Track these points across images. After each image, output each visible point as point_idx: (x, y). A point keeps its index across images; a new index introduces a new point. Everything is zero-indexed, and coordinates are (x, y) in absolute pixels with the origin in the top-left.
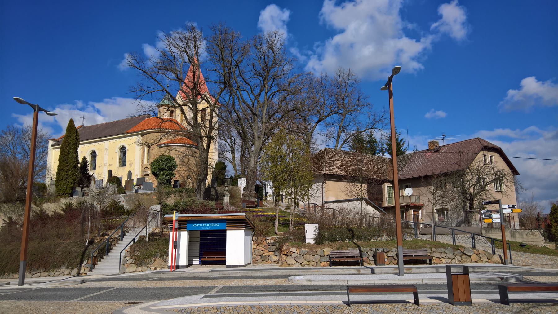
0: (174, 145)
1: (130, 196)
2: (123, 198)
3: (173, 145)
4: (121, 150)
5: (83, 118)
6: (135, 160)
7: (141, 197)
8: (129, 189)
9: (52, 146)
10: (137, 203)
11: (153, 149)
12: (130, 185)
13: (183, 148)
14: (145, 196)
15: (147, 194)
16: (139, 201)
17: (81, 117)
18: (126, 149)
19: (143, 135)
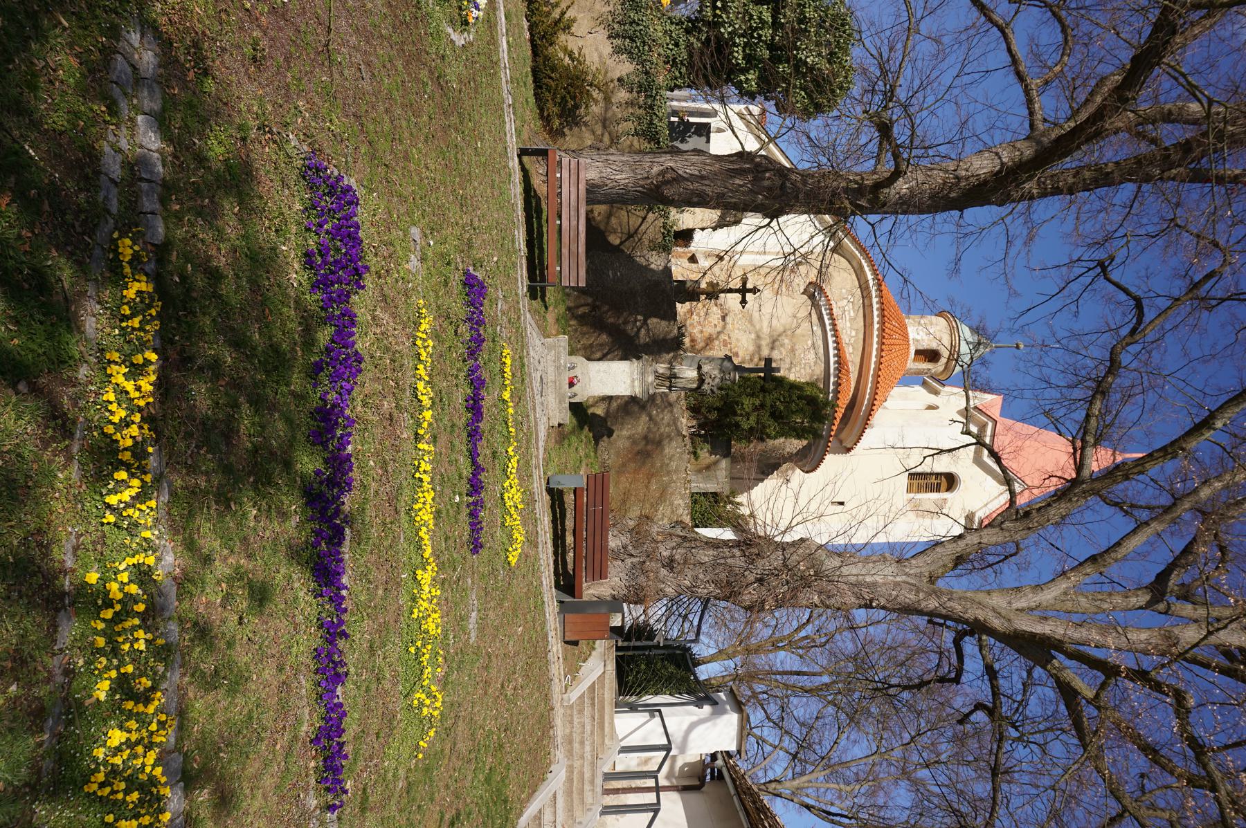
0: (828, 328)
3: (827, 322)
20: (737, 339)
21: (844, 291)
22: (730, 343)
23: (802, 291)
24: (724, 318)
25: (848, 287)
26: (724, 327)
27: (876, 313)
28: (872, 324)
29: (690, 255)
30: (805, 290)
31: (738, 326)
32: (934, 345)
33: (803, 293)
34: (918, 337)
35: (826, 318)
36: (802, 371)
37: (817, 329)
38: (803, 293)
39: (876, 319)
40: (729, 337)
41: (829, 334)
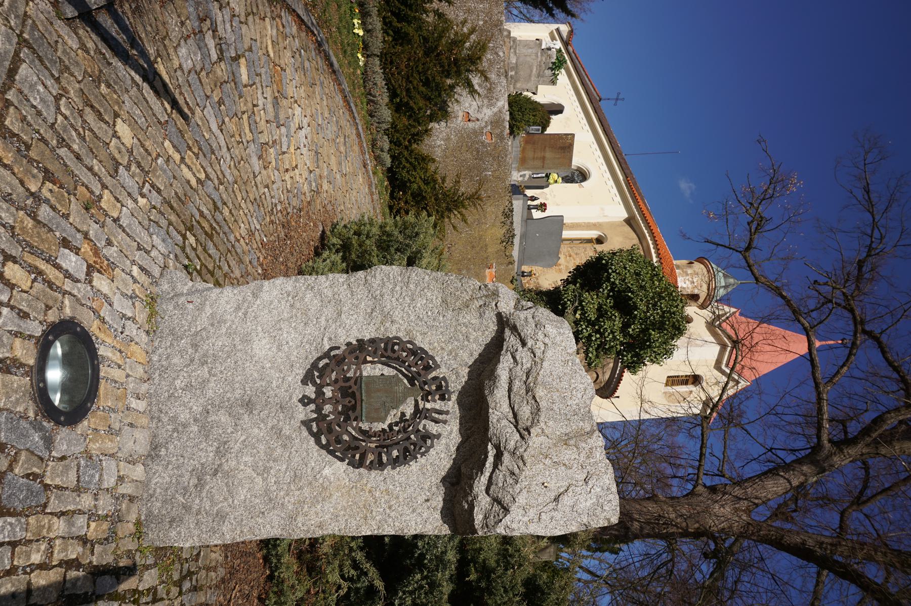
1: (499, 157)
2: (487, 113)
4: (577, 170)
5: (617, 99)
6: (557, 205)
7: (492, 211)
8: (530, 154)
9: (558, 30)
10: (464, 188)
12: (548, 154)
14: (500, 232)
15: (508, 239)
16: (475, 198)
17: (619, 94)
18: (581, 181)
19: (630, 222)
32: (696, 292)
34: (685, 286)
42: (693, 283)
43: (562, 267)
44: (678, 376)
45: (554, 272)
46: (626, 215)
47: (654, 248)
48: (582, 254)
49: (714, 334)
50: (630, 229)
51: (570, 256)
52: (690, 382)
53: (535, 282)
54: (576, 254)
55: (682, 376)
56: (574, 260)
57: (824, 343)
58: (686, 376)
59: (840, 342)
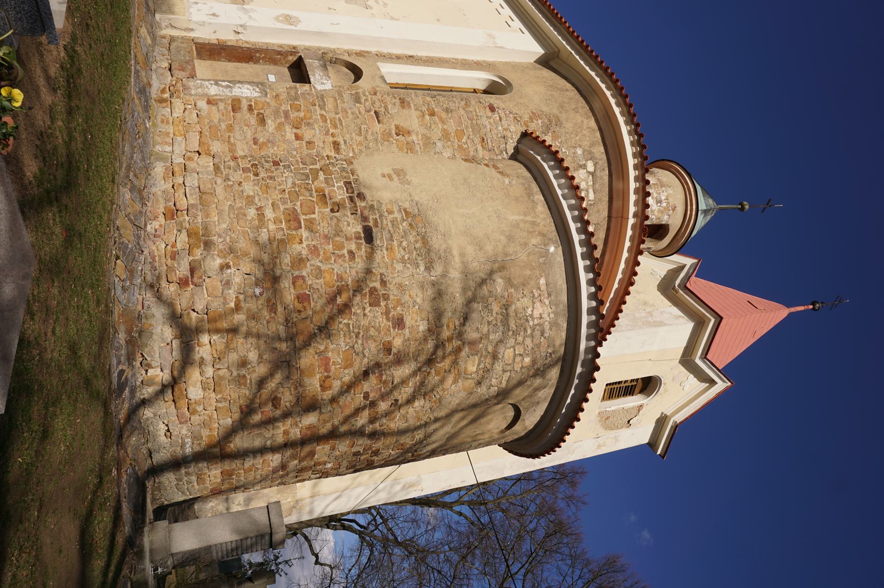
0: (579, 250)
3: (576, 238)
6: (392, 18)
11: (492, 109)
13: (554, 324)
20: (400, 286)
21: (579, 151)
22: (386, 297)
23: (511, 151)
24: (369, 235)
25: (586, 143)
26: (370, 257)
27: (633, 198)
28: (624, 218)
29: (292, 59)
30: (516, 149)
31: (399, 253)
32: (665, 220)
33: (513, 157)
35: (573, 226)
36: (528, 341)
37: (555, 250)
38: (513, 157)
39: (632, 209)
40: (383, 283)
41: (581, 264)
42: (660, 202)
43: (414, 137)
44: (620, 383)
45: (394, 148)
46: (539, 51)
47: (618, 105)
48: (462, 112)
49: (677, 302)
50: (553, 74)
51: (432, 114)
52: (637, 389)
53: (343, 170)
54: (447, 110)
55: (626, 382)
56: (443, 122)
57: (793, 310)
58: (632, 381)
59: (811, 307)
